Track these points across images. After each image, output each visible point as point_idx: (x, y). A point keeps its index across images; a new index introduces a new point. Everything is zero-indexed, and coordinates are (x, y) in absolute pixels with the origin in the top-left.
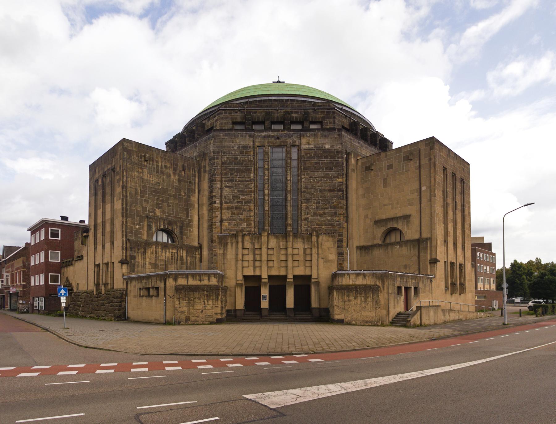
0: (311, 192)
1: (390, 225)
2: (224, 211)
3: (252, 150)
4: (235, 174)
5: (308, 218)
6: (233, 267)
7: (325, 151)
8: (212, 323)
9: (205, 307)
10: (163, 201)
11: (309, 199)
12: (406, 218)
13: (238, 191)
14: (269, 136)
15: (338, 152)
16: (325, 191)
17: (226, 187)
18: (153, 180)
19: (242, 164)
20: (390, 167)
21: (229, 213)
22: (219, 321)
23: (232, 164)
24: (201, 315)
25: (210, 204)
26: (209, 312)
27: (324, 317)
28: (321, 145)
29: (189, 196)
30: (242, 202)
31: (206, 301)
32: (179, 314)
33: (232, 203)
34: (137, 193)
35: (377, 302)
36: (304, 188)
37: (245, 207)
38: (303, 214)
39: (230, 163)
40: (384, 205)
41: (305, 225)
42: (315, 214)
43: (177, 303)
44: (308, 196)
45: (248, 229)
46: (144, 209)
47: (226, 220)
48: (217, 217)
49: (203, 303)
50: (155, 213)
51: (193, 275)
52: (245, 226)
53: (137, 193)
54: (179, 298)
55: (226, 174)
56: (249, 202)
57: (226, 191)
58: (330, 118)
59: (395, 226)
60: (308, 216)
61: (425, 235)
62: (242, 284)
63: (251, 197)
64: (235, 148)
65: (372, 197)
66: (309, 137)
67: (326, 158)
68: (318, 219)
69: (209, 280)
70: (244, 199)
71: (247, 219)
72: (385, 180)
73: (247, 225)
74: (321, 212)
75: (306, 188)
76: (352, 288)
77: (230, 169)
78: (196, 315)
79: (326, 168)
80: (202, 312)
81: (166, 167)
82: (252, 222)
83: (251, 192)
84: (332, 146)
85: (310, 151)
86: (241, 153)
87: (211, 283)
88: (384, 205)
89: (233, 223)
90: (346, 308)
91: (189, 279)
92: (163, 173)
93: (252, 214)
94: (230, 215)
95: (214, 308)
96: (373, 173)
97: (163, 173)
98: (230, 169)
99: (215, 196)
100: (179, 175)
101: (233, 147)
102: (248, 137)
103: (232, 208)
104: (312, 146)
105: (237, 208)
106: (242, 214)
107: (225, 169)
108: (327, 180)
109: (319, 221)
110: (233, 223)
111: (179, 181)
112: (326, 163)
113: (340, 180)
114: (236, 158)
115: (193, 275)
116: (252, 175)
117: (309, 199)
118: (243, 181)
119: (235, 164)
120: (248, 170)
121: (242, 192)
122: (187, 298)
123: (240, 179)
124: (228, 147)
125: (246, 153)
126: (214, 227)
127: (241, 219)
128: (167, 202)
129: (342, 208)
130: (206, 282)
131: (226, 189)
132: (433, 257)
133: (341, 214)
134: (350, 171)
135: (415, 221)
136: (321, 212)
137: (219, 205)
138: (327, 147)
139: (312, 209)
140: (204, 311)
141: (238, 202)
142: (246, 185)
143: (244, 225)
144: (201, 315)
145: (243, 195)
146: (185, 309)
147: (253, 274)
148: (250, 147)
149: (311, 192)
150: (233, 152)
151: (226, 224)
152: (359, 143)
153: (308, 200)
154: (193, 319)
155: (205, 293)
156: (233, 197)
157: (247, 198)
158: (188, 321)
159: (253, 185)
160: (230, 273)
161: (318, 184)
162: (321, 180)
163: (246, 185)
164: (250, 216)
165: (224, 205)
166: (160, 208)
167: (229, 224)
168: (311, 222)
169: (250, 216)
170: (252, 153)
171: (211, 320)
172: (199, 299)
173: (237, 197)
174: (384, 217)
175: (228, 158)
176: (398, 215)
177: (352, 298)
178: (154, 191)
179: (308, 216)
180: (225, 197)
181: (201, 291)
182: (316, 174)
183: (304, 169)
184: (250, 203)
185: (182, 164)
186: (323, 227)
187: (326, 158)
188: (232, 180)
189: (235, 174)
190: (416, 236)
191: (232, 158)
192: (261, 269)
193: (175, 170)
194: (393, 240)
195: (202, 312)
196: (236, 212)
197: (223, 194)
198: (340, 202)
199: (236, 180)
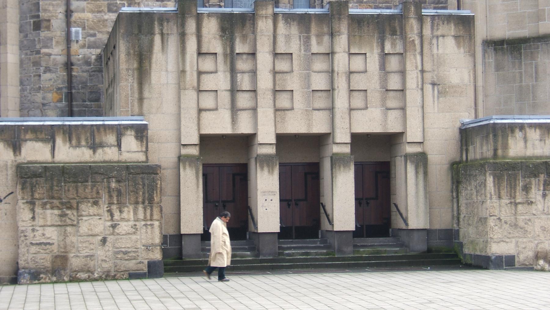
6: (169, 107)
8: (134, 276)
9: (114, 227)
22: (153, 271)
24: (101, 253)
26: (125, 244)
27: (445, 253)
31: (114, 207)
32: (33, 249)
43: (25, 214)
49: (107, 216)
51: (69, 133)
54: (32, 203)
69: (119, 146)
76: (536, 166)
78: (84, 253)
80: (104, 241)
87: (126, 157)
90: (521, 224)
91: (59, 141)
95: (139, 233)
115: (69, 133)
122: (56, 202)
130: (109, 154)
140: (110, 239)
144: (101, 253)
146: (52, 234)
154: (75, 262)
155: (113, 185)
158: (59, 270)
160: (159, 124)
171: (132, 265)
172: (96, 203)
181: (99, 178)
195: (104, 241)
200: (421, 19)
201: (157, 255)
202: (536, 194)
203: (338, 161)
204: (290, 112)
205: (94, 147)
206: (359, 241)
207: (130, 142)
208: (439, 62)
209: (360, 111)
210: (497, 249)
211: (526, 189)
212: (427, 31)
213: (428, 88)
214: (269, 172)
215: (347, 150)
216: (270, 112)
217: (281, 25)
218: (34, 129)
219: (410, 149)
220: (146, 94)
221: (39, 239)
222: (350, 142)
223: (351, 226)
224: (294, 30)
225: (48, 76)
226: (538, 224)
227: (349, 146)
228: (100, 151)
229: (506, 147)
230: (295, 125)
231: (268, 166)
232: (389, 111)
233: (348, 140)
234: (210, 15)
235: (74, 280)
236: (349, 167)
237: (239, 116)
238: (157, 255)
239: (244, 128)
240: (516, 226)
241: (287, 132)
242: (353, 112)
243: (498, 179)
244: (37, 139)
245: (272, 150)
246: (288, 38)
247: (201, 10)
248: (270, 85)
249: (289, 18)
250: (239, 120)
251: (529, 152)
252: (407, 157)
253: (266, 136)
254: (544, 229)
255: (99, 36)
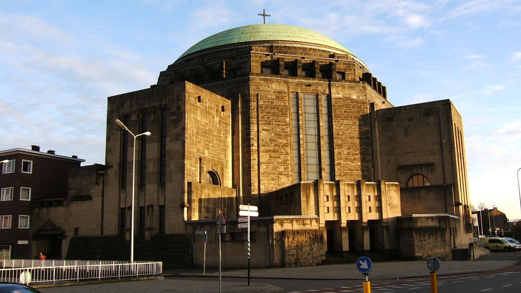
0: (342, 138)
1: (414, 172)
2: (261, 154)
3: (287, 95)
4: (272, 118)
5: (341, 163)
7: (352, 101)
8: (318, 264)
9: (312, 249)
10: (209, 142)
11: (341, 145)
12: (430, 166)
13: (275, 134)
14: (302, 83)
15: (363, 103)
16: (354, 138)
17: (263, 130)
18: (204, 121)
19: (278, 108)
20: (411, 119)
21: (266, 156)
23: (268, 108)
25: (246, 146)
26: (315, 255)
28: (348, 96)
29: (226, 138)
30: (279, 146)
33: (269, 146)
34: (193, 135)
35: (444, 241)
36: (336, 135)
37: (282, 151)
38: (336, 159)
39: (267, 107)
40: (407, 153)
41: (338, 170)
42: (346, 159)
44: (340, 142)
45: (285, 173)
46: (198, 149)
47: (264, 163)
48: (255, 159)
50: (204, 154)
52: (283, 170)
53: (193, 135)
55: (263, 118)
56: (285, 145)
57: (263, 135)
58: (351, 70)
59: (420, 172)
60: (340, 161)
61: (449, 181)
63: (287, 141)
64: (271, 93)
65: (394, 144)
66: (338, 87)
67: (354, 107)
68: (349, 165)
70: (281, 143)
71: (285, 162)
72: (406, 131)
73: (285, 169)
74: (352, 158)
75: (338, 134)
77: (267, 113)
79: (354, 117)
80: (309, 253)
81: (211, 107)
82: (289, 166)
83: (287, 136)
84: (358, 97)
85: (340, 100)
86: (277, 97)
88: (407, 153)
89: (271, 166)
92: (209, 114)
93: (289, 158)
94: (268, 158)
96: (394, 123)
97: (209, 114)
98: (267, 113)
99: (252, 139)
100: (220, 117)
101: (269, 92)
102: (282, 83)
103: (269, 151)
104: (341, 96)
105: (274, 151)
106: (279, 158)
107: (262, 113)
108: (355, 128)
109: (350, 166)
110: (271, 166)
111: (220, 121)
112: (354, 112)
113: (366, 128)
114: (273, 103)
116: (288, 119)
117: (341, 145)
118: (279, 125)
119: (271, 108)
120: (284, 115)
121: (279, 135)
123: (277, 123)
124: (264, 91)
125: (282, 98)
126: (252, 169)
127: (278, 163)
128: (212, 143)
129: (369, 154)
130: (308, 227)
131: (264, 132)
132: (457, 201)
133: (369, 160)
134: (373, 120)
135: (439, 169)
136: (352, 158)
137: (256, 148)
138: (354, 97)
139: (344, 154)
140: (311, 253)
141: (275, 145)
142: (282, 129)
143: (282, 169)
145: (280, 138)
147: (332, 219)
148: (285, 93)
149: (342, 138)
150: (269, 96)
151: (264, 167)
152: (374, 94)
153: (340, 146)
156: (271, 140)
157: (284, 141)
159: (289, 129)
161: (348, 132)
162: (350, 128)
163: (282, 129)
164: (287, 160)
165: (262, 148)
166: (208, 149)
167: (267, 167)
168: (343, 167)
169: (287, 160)
170: (287, 98)
171: (317, 261)
173: (273, 140)
174: (407, 163)
175: (264, 102)
176: (422, 163)
177: (426, 238)
178: (205, 133)
179: (340, 161)
180: (263, 139)
182: (345, 121)
183: (335, 116)
184: (287, 146)
185: (221, 105)
186: (354, 172)
187: (354, 107)
188: (269, 124)
189: (272, 118)
190: (440, 182)
191: (269, 102)
193: (217, 111)
194: (416, 185)
196: (273, 155)
197: (260, 137)
198: (368, 149)
199: (273, 123)
200: (385, 185)
201: (324, 258)
202: (426, 238)
203: (363, 228)
205: (304, 225)
207: (314, 223)
208: (390, 198)
210: (418, 254)
211: (424, 236)
212: (387, 189)
213: (388, 206)
215: (366, 225)
216: (345, 213)
217: (346, 187)
218: (287, 219)
219: (384, 225)
220: (309, 208)
221: (291, 253)
224: (350, 188)
225: (254, 201)
226: (428, 247)
228: (305, 226)
229: (417, 223)
234: (326, 184)
235: (301, 266)
238: (324, 258)
240: (421, 247)
243: (416, 233)
244: (288, 223)
246: (348, 191)
247: (324, 182)
248: (344, 205)
249: (348, 185)
251: (423, 225)
252: (383, 227)
254: (429, 248)
255: (269, 188)
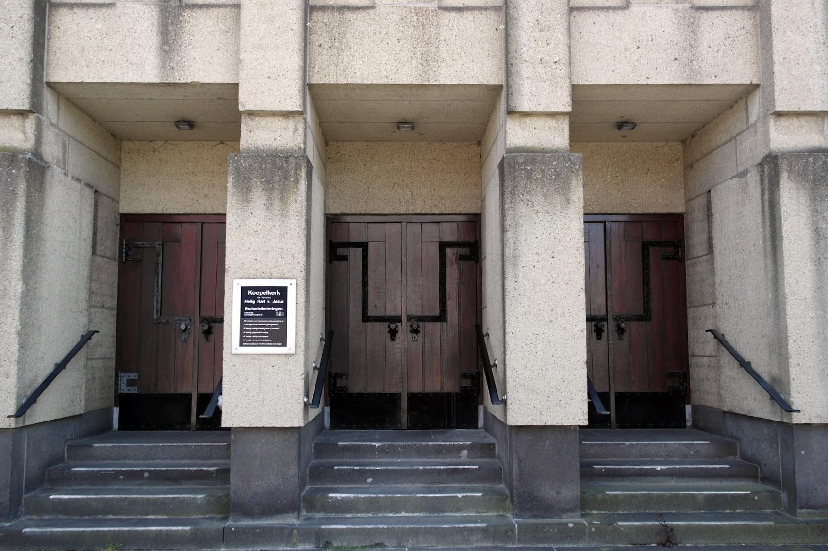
62: (36, 167)
192: (237, 20)
204: (360, 14)
206: (595, 444)
209: (602, 14)
214: (270, 206)
222: (569, 109)
223: (574, 411)
227: (565, 124)
230: (376, 58)
231: (268, 187)
232: (705, 15)
233: (563, 104)
236: (564, 191)
237: (187, 27)
239: (203, 62)
241: (350, 81)
242: (580, 18)
245: (287, 136)
250: (186, 38)
253: (270, 83)
